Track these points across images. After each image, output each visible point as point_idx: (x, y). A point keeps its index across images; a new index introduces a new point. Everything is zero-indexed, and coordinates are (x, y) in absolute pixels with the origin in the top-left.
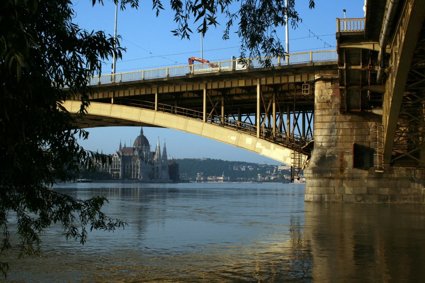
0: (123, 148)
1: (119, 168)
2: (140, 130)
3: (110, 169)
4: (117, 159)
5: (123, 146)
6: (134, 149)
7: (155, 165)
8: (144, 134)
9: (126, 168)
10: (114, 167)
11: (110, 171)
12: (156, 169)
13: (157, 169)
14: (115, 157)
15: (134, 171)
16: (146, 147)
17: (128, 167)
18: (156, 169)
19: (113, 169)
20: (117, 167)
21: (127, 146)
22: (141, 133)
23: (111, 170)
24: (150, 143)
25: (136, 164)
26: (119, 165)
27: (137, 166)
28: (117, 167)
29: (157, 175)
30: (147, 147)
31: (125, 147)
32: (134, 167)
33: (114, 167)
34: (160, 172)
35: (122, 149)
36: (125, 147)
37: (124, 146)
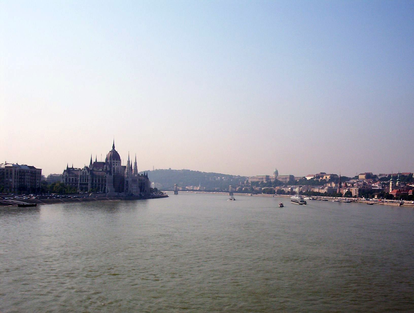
1: (88, 182)
2: (113, 145)
3: (79, 182)
4: (86, 174)
5: (94, 161)
6: (103, 163)
9: (94, 182)
10: (83, 181)
11: (79, 185)
13: (127, 183)
15: (102, 185)
16: (117, 161)
17: (96, 181)
19: (82, 182)
20: (85, 181)
21: (98, 161)
22: (113, 148)
23: (80, 184)
24: (121, 158)
25: (103, 178)
26: (88, 179)
27: (105, 180)
28: (85, 181)
29: (127, 189)
30: (118, 161)
31: (96, 161)
32: (102, 181)
33: (83, 181)
34: (129, 186)
36: (96, 161)
37: (95, 161)
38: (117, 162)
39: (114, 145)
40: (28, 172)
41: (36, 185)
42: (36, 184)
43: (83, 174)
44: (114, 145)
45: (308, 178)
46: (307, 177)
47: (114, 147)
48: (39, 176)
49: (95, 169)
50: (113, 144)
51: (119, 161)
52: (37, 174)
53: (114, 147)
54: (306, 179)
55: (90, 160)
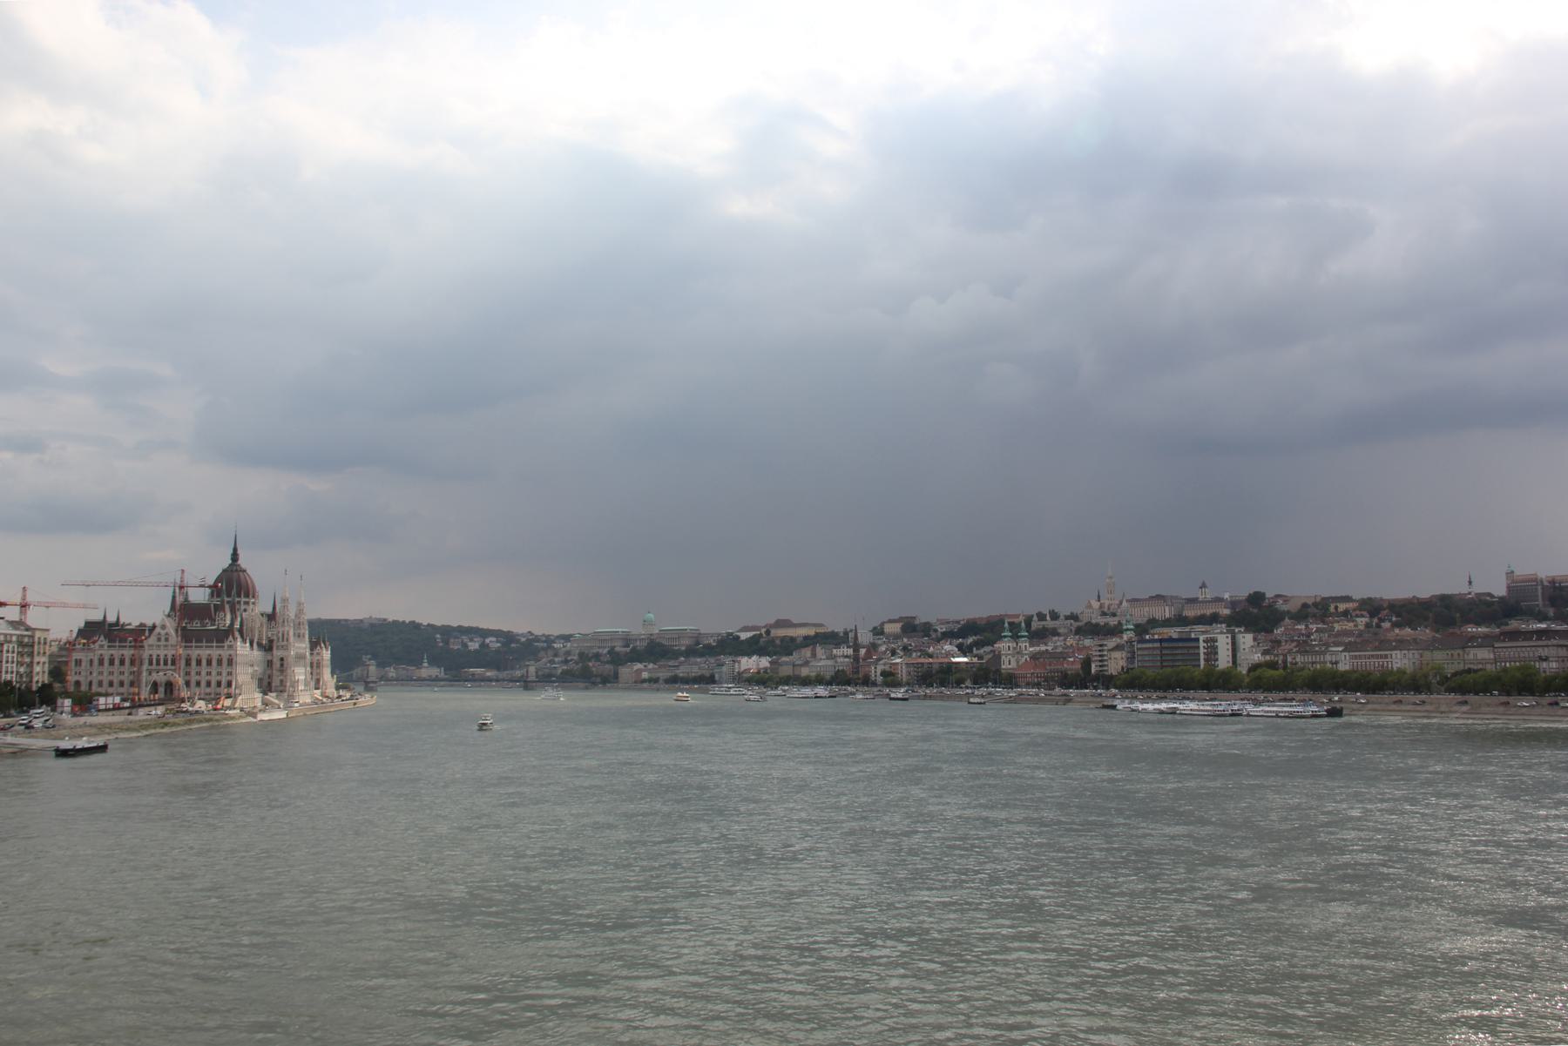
0: (181, 605)
2: (232, 551)
4: (167, 640)
5: (179, 600)
7: (275, 651)
8: (243, 562)
12: (277, 664)
13: (282, 665)
14: (163, 632)
16: (247, 600)
18: (277, 664)
22: (232, 559)
29: (282, 681)
31: (186, 599)
35: (178, 607)
38: (247, 603)
39: (235, 550)
40: (10, 642)
41: (31, 681)
42: (32, 677)
43: (159, 640)
44: (235, 550)
45: (744, 636)
46: (738, 631)
47: (235, 556)
48: (42, 652)
49: (199, 625)
50: (232, 546)
51: (253, 600)
52: (36, 647)
53: (235, 556)
54: (738, 637)
55: (171, 598)
